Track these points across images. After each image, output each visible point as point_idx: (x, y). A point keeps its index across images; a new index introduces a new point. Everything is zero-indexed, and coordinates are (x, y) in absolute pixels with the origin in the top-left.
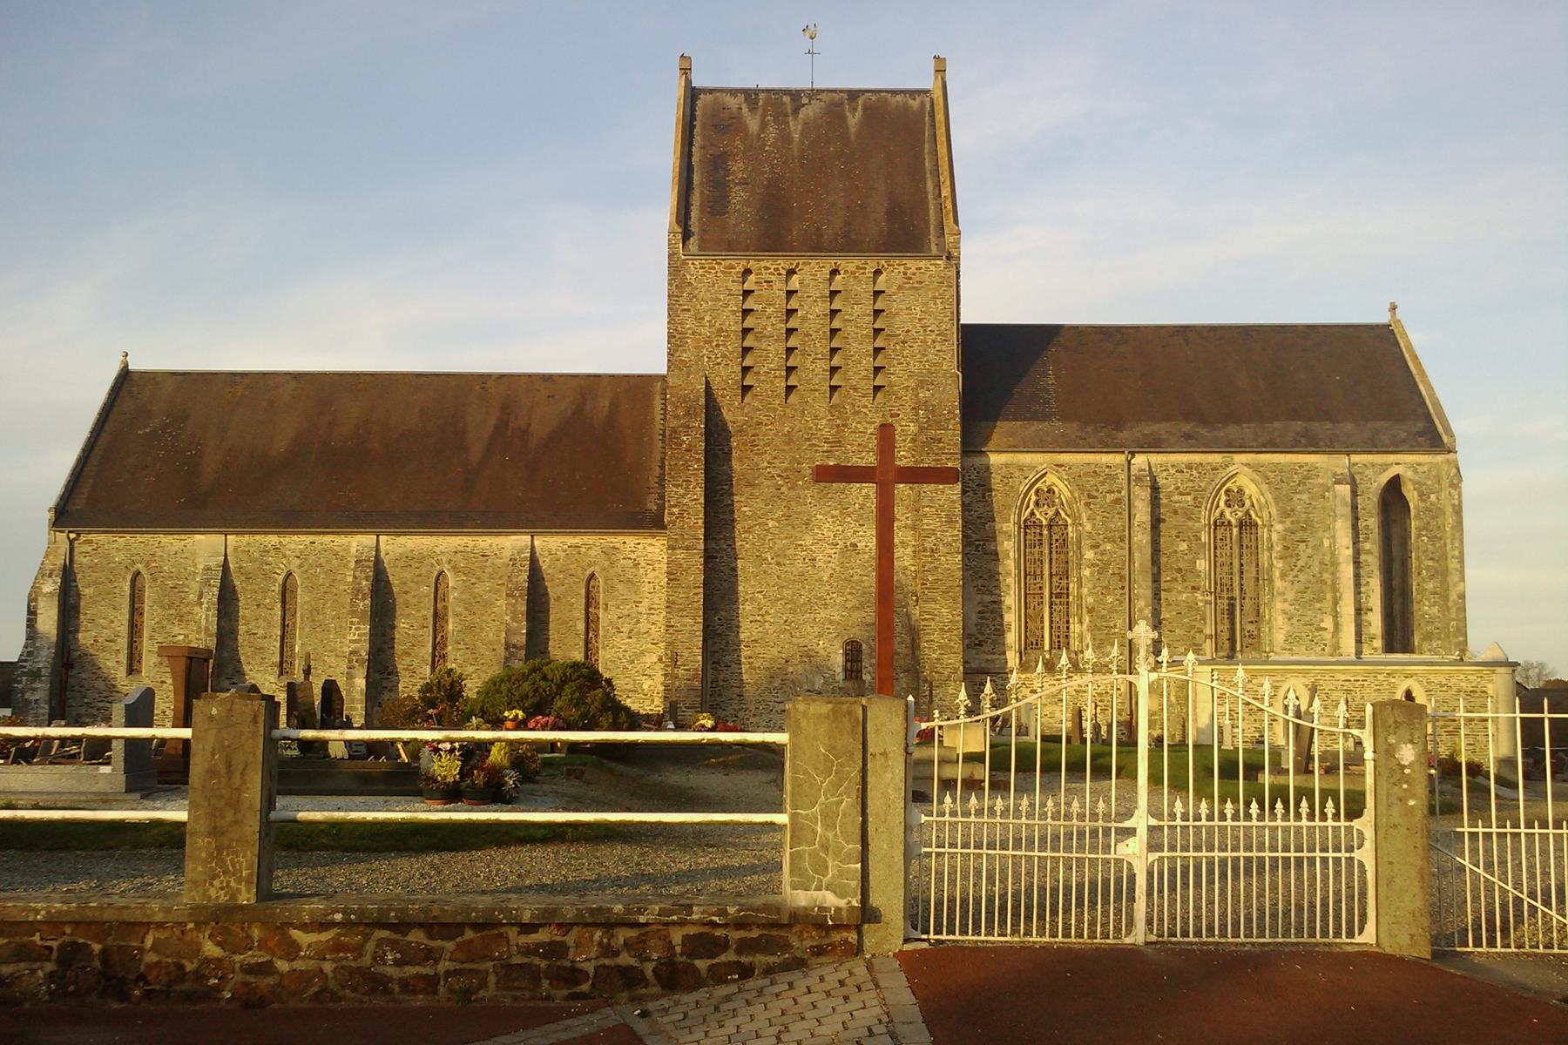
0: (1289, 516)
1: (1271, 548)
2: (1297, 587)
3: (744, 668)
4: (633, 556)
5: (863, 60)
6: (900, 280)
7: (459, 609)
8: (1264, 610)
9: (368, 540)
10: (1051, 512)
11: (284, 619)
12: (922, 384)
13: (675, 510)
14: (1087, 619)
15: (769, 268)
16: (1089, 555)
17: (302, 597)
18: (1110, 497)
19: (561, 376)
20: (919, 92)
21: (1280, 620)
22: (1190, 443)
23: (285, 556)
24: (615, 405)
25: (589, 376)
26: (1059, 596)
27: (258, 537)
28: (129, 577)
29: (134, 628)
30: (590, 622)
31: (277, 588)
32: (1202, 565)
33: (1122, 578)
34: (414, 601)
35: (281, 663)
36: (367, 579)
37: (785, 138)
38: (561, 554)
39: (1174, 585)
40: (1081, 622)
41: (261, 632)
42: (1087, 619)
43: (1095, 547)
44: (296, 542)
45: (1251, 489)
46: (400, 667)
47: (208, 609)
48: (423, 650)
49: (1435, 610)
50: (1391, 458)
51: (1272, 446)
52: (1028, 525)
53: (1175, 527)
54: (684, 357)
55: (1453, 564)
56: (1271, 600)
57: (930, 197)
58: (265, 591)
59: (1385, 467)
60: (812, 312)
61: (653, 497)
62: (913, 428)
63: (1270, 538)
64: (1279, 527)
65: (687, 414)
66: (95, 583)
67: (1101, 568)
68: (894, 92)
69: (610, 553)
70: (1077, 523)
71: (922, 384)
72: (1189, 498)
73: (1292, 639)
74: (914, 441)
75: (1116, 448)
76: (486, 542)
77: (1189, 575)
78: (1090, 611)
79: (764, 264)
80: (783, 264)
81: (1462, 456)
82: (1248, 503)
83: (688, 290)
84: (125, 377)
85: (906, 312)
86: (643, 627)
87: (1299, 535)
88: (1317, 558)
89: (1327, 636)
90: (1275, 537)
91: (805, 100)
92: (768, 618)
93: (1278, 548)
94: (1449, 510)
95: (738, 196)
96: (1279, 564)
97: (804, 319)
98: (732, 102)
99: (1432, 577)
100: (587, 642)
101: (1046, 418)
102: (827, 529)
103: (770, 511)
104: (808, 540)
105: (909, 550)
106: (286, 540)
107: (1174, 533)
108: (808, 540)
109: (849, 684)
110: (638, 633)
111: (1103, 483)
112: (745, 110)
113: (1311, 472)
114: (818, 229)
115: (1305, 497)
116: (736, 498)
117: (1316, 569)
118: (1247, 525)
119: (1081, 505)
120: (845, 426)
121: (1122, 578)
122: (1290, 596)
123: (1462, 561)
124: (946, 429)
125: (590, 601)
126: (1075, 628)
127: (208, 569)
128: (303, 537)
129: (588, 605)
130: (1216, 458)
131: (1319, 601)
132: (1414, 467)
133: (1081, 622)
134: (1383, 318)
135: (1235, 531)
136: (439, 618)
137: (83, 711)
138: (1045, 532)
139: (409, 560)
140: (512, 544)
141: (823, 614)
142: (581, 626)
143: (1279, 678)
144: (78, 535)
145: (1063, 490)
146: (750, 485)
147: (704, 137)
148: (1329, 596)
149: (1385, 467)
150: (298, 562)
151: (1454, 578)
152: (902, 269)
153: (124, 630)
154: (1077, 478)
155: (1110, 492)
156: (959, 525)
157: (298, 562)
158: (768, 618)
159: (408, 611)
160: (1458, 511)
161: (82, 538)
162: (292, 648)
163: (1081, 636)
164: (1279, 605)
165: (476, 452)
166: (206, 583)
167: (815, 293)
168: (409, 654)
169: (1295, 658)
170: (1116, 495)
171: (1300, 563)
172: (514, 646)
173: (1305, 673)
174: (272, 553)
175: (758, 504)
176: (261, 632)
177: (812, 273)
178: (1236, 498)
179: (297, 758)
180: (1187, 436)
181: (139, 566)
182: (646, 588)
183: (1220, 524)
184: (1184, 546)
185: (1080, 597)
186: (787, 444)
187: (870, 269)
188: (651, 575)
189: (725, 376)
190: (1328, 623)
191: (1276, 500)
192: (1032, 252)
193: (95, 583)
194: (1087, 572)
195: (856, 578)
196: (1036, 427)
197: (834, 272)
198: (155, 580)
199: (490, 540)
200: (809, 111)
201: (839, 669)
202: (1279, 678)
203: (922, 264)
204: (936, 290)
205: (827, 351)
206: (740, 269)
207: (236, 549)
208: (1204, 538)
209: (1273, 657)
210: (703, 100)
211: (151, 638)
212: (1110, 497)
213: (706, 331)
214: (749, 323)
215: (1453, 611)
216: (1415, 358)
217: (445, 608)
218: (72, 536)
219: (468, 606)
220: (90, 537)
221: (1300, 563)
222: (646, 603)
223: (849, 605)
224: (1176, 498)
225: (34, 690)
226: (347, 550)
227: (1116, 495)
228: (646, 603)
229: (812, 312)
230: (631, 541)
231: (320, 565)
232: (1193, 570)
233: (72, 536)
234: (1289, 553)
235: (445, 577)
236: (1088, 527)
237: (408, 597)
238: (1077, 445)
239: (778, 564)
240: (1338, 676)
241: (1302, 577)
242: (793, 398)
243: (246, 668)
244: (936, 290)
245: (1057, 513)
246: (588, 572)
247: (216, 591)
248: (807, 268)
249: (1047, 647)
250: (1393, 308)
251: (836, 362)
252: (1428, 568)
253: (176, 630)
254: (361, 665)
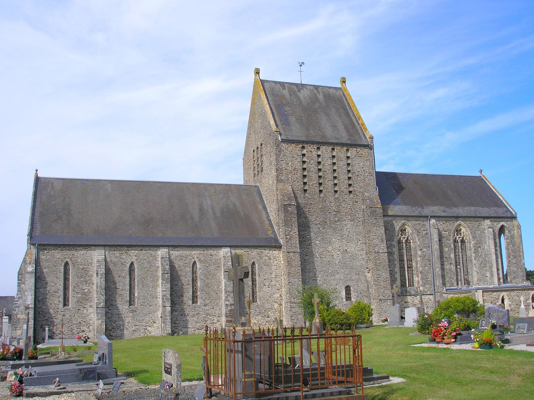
1: (471, 250)
2: (480, 262)
4: (268, 255)
14: (420, 275)
18: (424, 232)
21: (475, 274)
23: (130, 255)
28: (63, 264)
31: (127, 269)
33: (430, 261)
42: (420, 275)
43: (421, 250)
47: (101, 278)
48: (189, 294)
56: (472, 267)
60: (327, 163)
63: (470, 246)
64: (473, 242)
65: (289, 200)
66: (48, 267)
67: (423, 257)
68: (330, 88)
72: (447, 233)
73: (479, 280)
78: (421, 273)
83: (283, 152)
84: (37, 179)
86: (273, 283)
88: (484, 253)
90: (472, 246)
93: (473, 249)
97: (323, 165)
99: (514, 258)
100: (253, 290)
104: (330, 248)
108: (330, 248)
110: (272, 285)
111: (422, 227)
115: (479, 232)
117: (484, 256)
119: (415, 235)
120: (340, 205)
121: (430, 261)
122: (477, 265)
123: (523, 253)
126: (416, 279)
127: (98, 261)
131: (485, 267)
134: (478, 174)
139: (181, 257)
150: (136, 258)
153: (61, 288)
155: (424, 230)
163: (418, 282)
170: (426, 232)
171: (479, 254)
172: (229, 292)
185: (417, 268)
186: (321, 212)
189: (299, 185)
195: (347, 262)
211: (73, 291)
212: (424, 232)
213: (290, 169)
214: (305, 166)
217: (196, 277)
221: (479, 254)
223: (346, 273)
224: (443, 232)
227: (426, 232)
229: (327, 163)
231: (145, 260)
234: (476, 251)
236: (418, 243)
242: (322, 195)
246: (252, 261)
251: (336, 182)
252: (513, 255)
253: (84, 287)
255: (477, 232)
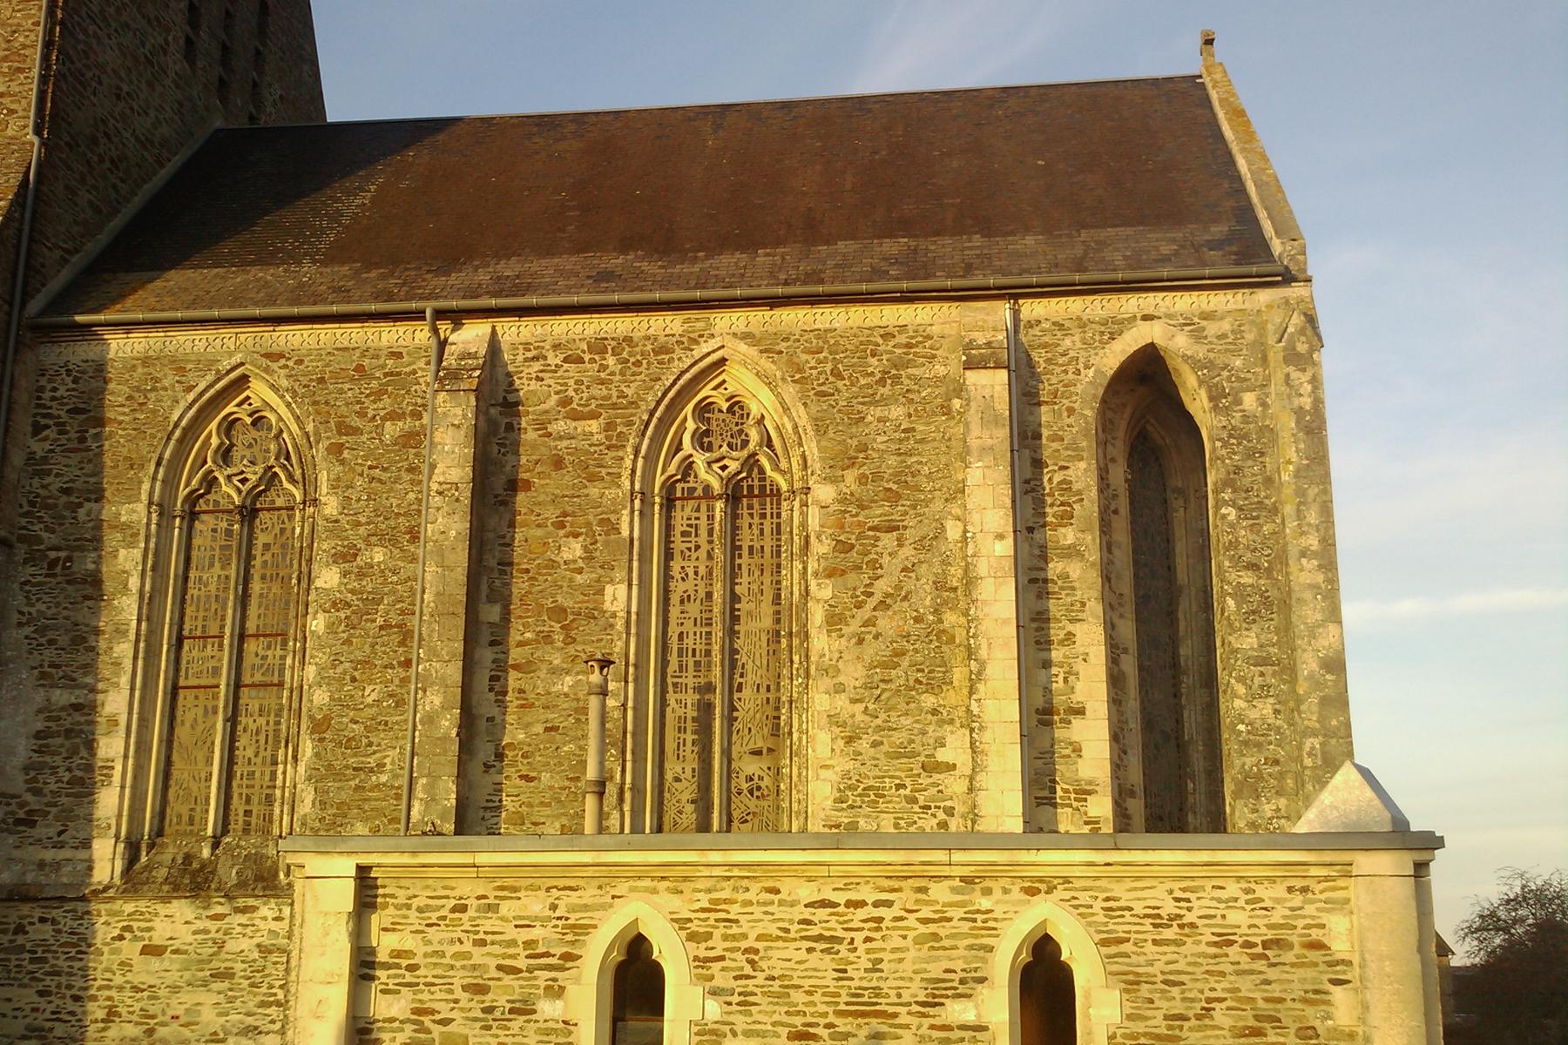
2: (872, 650)
16: (328, 578)
18: (391, 430)
32: (617, 597)
43: (345, 556)
45: (761, 400)
50: (1131, 303)
55: (1305, 574)
63: (804, 525)
72: (594, 426)
73: (852, 793)
78: (320, 727)
82: (754, 436)
90: (814, 522)
93: (821, 548)
94: (1287, 424)
96: (823, 591)
99: (1252, 617)
107: (551, 514)
111: (378, 395)
113: (918, 344)
115: (897, 412)
117: (925, 600)
122: (853, 674)
123: (1328, 564)
131: (931, 688)
132: (1191, 325)
149: (1114, 328)
151: (1308, 612)
154: (313, 387)
155: (393, 416)
160: (1313, 427)
164: (821, 700)
171: (882, 587)
184: (574, 550)
191: (820, 428)
212: (391, 430)
221: (882, 587)
224: (560, 426)
232: (594, 613)
234: (851, 557)
241: (885, 623)
252: (1240, 593)
255: (872, 414)
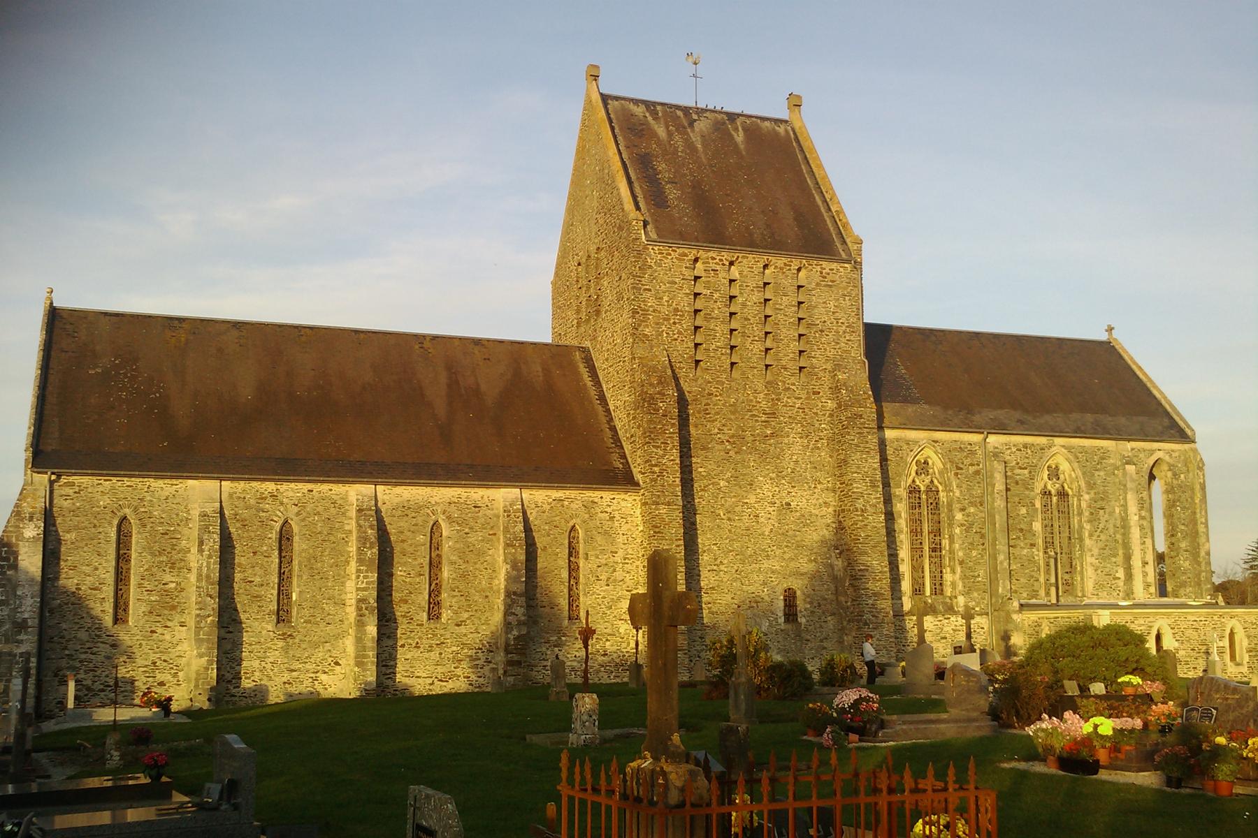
0: (1092, 488)
1: (1080, 514)
2: (1101, 544)
3: (705, 612)
4: (609, 510)
5: (742, 88)
6: (817, 278)
7: (454, 558)
8: (1077, 563)
9: (366, 489)
10: (927, 481)
11: (280, 567)
12: (837, 367)
13: (656, 469)
14: (958, 569)
15: (713, 258)
16: (959, 516)
17: (299, 544)
18: (972, 469)
19: (488, 340)
20: (782, 121)
21: (1089, 572)
22: (1023, 427)
23: (282, 504)
24: (547, 371)
25: (513, 343)
26: (934, 550)
27: (254, 484)
28: (116, 522)
29: (121, 577)
30: (573, 570)
31: (274, 535)
32: (1037, 526)
33: (983, 536)
34: (411, 550)
35: (278, 610)
36: (371, 527)
37: (690, 146)
38: (547, 507)
39: (1018, 542)
40: (953, 571)
41: (257, 579)
42: (958, 569)
43: (963, 510)
44: (292, 490)
45: (1065, 467)
46: (398, 614)
47: (210, 557)
48: (420, 598)
49: (1187, 563)
50: (1156, 445)
51: (1079, 432)
52: (913, 491)
53: (1018, 495)
54: (647, 331)
55: (1201, 529)
56: (1081, 555)
57: (823, 210)
58: (262, 538)
59: (1152, 452)
60: (749, 299)
61: (615, 457)
62: (831, 405)
64: (1087, 497)
65: (660, 383)
66: (77, 528)
67: (968, 527)
68: (764, 119)
69: (589, 506)
70: (948, 489)
71: (837, 367)
72: (1026, 472)
73: (1099, 586)
74: (831, 415)
75: (977, 429)
76: (478, 494)
77: (1028, 535)
78: (961, 563)
79: (711, 254)
80: (726, 256)
81: (1199, 445)
82: (1062, 476)
83: (649, 272)
85: (824, 306)
86: (619, 574)
87: (1099, 505)
88: (1112, 522)
89: (1121, 583)
90: (1084, 505)
91: (695, 117)
92: (722, 567)
93: (1087, 514)
94: (1198, 487)
95: (672, 193)
96: (1087, 526)
97: (744, 305)
98: (639, 111)
100: (570, 590)
101: (914, 401)
102: (767, 489)
103: (722, 472)
104: (752, 499)
105: (831, 510)
106: (284, 487)
107: (1017, 499)
108: (752, 499)
109: (789, 626)
110: (615, 581)
111: (966, 457)
112: (650, 118)
113: (1105, 455)
114: (747, 228)
115: (1102, 473)
116: (694, 460)
117: (1111, 531)
118: (1063, 494)
119: (951, 475)
120: (778, 400)
121: (983, 536)
122: (1096, 552)
124: (866, 407)
125: (572, 551)
126: (948, 577)
127: (204, 515)
128: (300, 485)
129: (570, 555)
130: (1043, 440)
132: (1170, 453)
133: (953, 571)
134: (1103, 337)
135: (1055, 499)
136: (435, 565)
137: (64, 663)
138: (924, 496)
139: (406, 509)
140: (501, 496)
141: (766, 565)
142: (565, 574)
143: (1151, 619)
144: (59, 476)
145: (936, 462)
146: (704, 448)
147: (624, 138)
148: (1121, 552)
149: (1152, 452)
150: (296, 509)
151: (1202, 540)
152: (819, 268)
153: (110, 578)
154: (949, 453)
155: (972, 465)
156: (880, 489)
157: (296, 509)
158: (722, 567)
159: (405, 559)
160: (1203, 487)
161: (64, 480)
162: (289, 597)
163: (953, 584)
164: (1089, 559)
165: (441, 407)
166: (205, 529)
167: (752, 284)
168: (406, 602)
169: (1101, 601)
170: (976, 468)
171: (1101, 526)
172: (515, 593)
173: (1169, 615)
174: (270, 500)
175: (711, 466)
176: (257, 579)
177: (748, 266)
178: (1054, 473)
179: (1001, 762)
180: (1021, 422)
181: (127, 511)
182: (621, 539)
183: (1046, 493)
184: (1023, 511)
185: (951, 551)
186: (733, 413)
187: (794, 267)
188: (625, 527)
189: (683, 348)
190: (1121, 573)
192: (927, 260)
193: (77, 528)
194: (957, 531)
195: (791, 533)
196: (911, 409)
197: (765, 267)
198: (144, 526)
199: (481, 492)
200: (702, 125)
201: (781, 614)
202: (1151, 619)
203: (834, 266)
204: (845, 288)
205: (762, 334)
206: (692, 257)
207: (231, 495)
208: (1038, 505)
209: (1086, 601)
210: (613, 104)
211: (140, 586)
212: (972, 469)
213: (665, 310)
214: (698, 305)
215: (1203, 565)
216: (1140, 368)
217: (439, 556)
218: (53, 477)
219: (462, 555)
220: (71, 479)
221: (1101, 526)
222: (621, 553)
223: (787, 556)
224: (1017, 471)
225: (21, 642)
226: (345, 498)
227: (976, 468)
228: (621, 553)
229: (749, 299)
230: (607, 495)
231: (318, 514)
232: (1030, 531)
233: (53, 477)
234: (1094, 519)
235: (439, 527)
236: (958, 494)
237: (405, 545)
238: (948, 425)
239: (729, 519)
240: (1190, 618)
241: (1103, 537)
242: (736, 374)
243: (243, 617)
244: (845, 288)
245: (932, 482)
246: (571, 524)
247: (217, 537)
248: (745, 261)
249: (928, 593)
250: (1110, 329)
251: (769, 344)
252: (1182, 531)
253: (167, 578)
254: (371, 613)
255: (1097, 473)
